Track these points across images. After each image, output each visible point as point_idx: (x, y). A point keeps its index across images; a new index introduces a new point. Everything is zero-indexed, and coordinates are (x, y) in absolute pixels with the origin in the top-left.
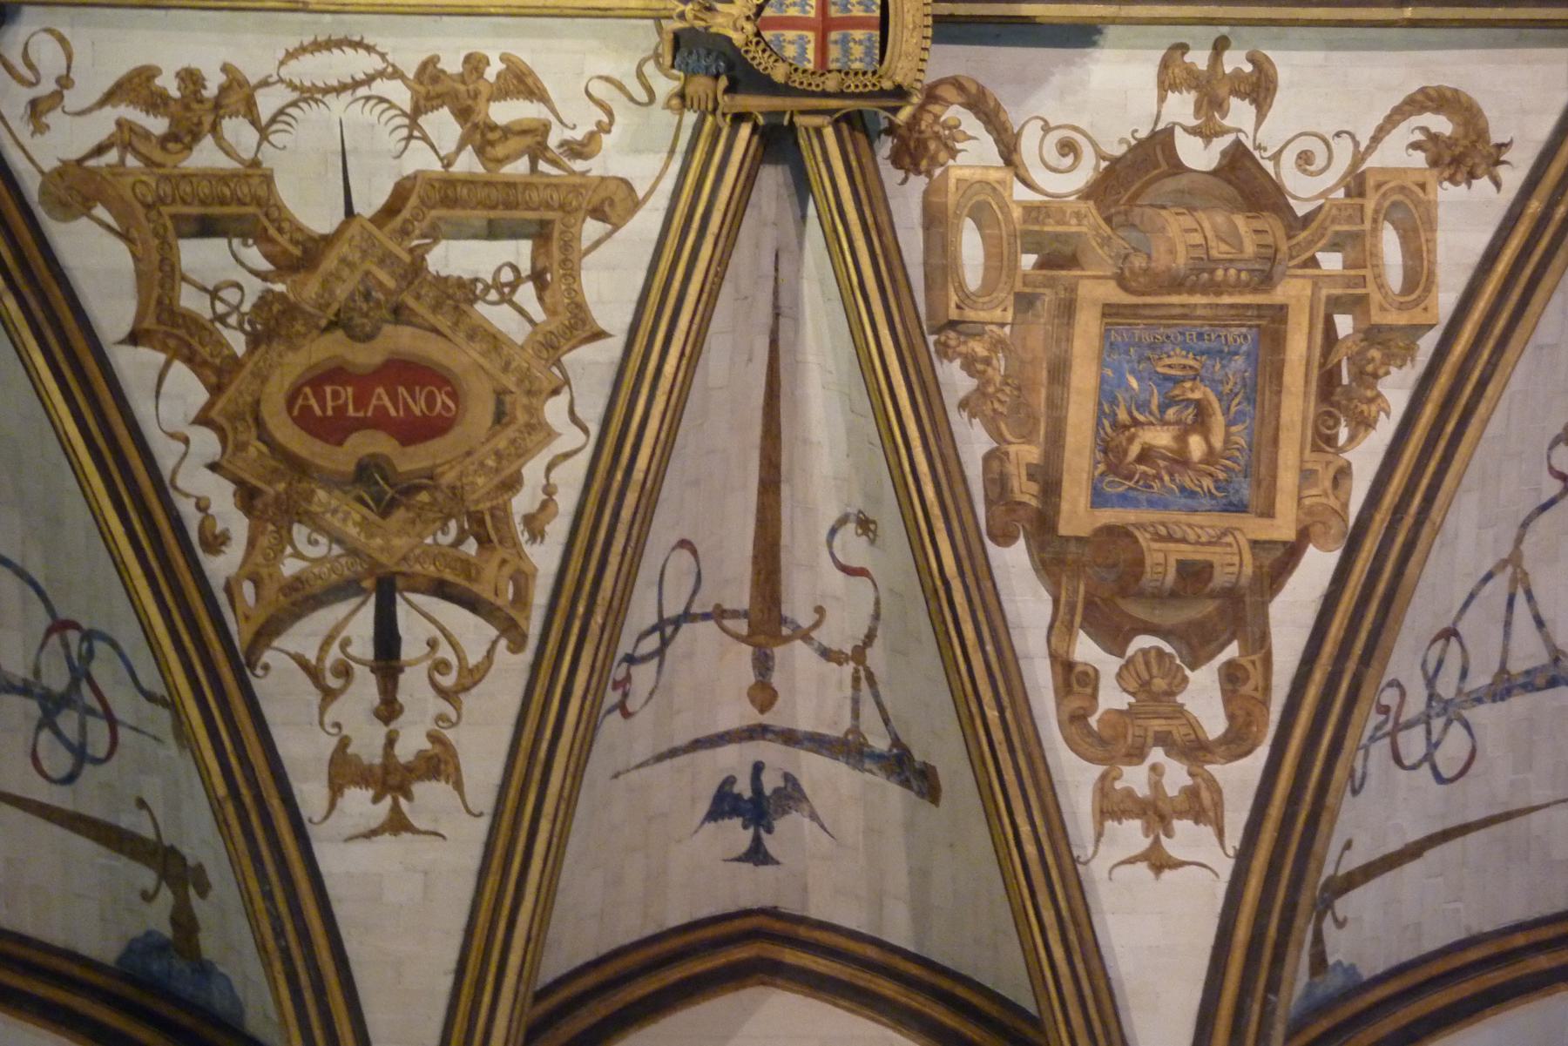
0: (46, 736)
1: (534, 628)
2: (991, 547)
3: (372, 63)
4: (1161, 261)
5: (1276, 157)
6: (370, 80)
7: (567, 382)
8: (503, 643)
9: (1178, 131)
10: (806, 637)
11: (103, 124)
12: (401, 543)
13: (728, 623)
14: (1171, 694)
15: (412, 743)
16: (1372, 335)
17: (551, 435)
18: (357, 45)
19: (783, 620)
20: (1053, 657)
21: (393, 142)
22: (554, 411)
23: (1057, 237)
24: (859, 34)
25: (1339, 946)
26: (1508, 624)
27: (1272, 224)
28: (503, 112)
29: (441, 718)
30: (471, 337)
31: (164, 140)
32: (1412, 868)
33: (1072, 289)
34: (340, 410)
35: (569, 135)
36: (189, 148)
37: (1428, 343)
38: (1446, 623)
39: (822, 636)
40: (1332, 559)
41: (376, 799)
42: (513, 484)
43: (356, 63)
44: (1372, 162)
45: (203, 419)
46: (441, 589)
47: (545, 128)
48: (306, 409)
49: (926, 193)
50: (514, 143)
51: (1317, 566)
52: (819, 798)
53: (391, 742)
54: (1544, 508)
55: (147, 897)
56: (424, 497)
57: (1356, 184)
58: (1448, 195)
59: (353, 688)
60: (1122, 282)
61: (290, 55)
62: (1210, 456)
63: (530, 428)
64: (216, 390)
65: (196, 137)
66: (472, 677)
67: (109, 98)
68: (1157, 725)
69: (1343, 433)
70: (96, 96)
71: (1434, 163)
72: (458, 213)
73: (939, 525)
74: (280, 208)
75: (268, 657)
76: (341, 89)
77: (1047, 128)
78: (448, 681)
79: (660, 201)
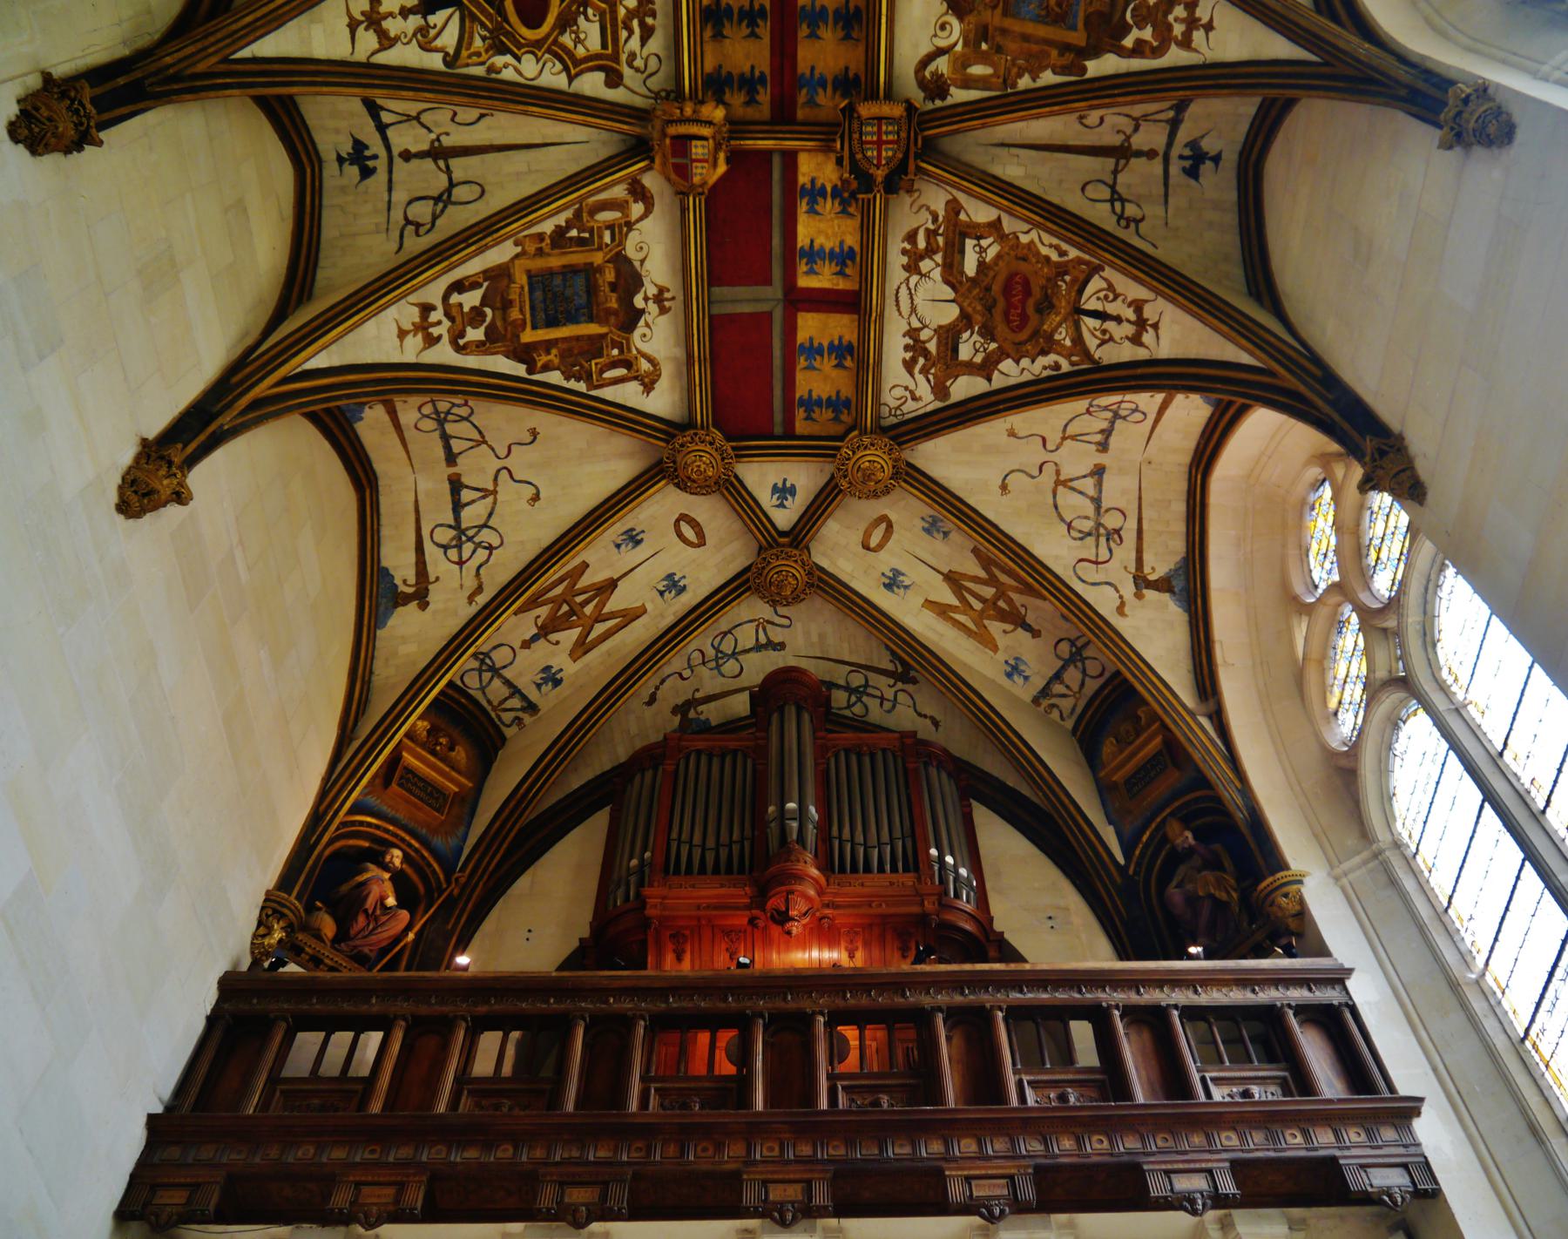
0: (1128, 418)
3: (904, 286)
6: (909, 289)
7: (1014, 233)
8: (1101, 273)
10: (1128, 138)
11: (920, 378)
12: (1063, 304)
13: (1120, 168)
15: (1130, 314)
17: (1032, 242)
19: (1122, 145)
20: (1130, 57)
21: (930, 283)
22: (1024, 239)
23: (976, 34)
24: (884, 128)
28: (922, 244)
29: (1123, 301)
30: (997, 265)
31: (926, 360)
33: (996, 29)
34: (1019, 315)
35: (930, 221)
36: (929, 352)
39: (1129, 131)
41: (1147, 331)
42: (1047, 259)
43: (904, 292)
45: (1017, 362)
46: (1081, 291)
47: (927, 230)
48: (1017, 326)
49: (957, 87)
50: (932, 240)
52: (1197, 134)
56: (1049, 291)
59: (1110, 330)
60: (994, 7)
61: (900, 314)
63: (1029, 249)
64: (1008, 356)
65: (926, 349)
66: (1111, 287)
68: (1160, 15)
70: (911, 379)
72: (956, 263)
74: (950, 324)
75: (1096, 357)
77: (935, 35)
78: (1111, 296)
79: (954, 192)
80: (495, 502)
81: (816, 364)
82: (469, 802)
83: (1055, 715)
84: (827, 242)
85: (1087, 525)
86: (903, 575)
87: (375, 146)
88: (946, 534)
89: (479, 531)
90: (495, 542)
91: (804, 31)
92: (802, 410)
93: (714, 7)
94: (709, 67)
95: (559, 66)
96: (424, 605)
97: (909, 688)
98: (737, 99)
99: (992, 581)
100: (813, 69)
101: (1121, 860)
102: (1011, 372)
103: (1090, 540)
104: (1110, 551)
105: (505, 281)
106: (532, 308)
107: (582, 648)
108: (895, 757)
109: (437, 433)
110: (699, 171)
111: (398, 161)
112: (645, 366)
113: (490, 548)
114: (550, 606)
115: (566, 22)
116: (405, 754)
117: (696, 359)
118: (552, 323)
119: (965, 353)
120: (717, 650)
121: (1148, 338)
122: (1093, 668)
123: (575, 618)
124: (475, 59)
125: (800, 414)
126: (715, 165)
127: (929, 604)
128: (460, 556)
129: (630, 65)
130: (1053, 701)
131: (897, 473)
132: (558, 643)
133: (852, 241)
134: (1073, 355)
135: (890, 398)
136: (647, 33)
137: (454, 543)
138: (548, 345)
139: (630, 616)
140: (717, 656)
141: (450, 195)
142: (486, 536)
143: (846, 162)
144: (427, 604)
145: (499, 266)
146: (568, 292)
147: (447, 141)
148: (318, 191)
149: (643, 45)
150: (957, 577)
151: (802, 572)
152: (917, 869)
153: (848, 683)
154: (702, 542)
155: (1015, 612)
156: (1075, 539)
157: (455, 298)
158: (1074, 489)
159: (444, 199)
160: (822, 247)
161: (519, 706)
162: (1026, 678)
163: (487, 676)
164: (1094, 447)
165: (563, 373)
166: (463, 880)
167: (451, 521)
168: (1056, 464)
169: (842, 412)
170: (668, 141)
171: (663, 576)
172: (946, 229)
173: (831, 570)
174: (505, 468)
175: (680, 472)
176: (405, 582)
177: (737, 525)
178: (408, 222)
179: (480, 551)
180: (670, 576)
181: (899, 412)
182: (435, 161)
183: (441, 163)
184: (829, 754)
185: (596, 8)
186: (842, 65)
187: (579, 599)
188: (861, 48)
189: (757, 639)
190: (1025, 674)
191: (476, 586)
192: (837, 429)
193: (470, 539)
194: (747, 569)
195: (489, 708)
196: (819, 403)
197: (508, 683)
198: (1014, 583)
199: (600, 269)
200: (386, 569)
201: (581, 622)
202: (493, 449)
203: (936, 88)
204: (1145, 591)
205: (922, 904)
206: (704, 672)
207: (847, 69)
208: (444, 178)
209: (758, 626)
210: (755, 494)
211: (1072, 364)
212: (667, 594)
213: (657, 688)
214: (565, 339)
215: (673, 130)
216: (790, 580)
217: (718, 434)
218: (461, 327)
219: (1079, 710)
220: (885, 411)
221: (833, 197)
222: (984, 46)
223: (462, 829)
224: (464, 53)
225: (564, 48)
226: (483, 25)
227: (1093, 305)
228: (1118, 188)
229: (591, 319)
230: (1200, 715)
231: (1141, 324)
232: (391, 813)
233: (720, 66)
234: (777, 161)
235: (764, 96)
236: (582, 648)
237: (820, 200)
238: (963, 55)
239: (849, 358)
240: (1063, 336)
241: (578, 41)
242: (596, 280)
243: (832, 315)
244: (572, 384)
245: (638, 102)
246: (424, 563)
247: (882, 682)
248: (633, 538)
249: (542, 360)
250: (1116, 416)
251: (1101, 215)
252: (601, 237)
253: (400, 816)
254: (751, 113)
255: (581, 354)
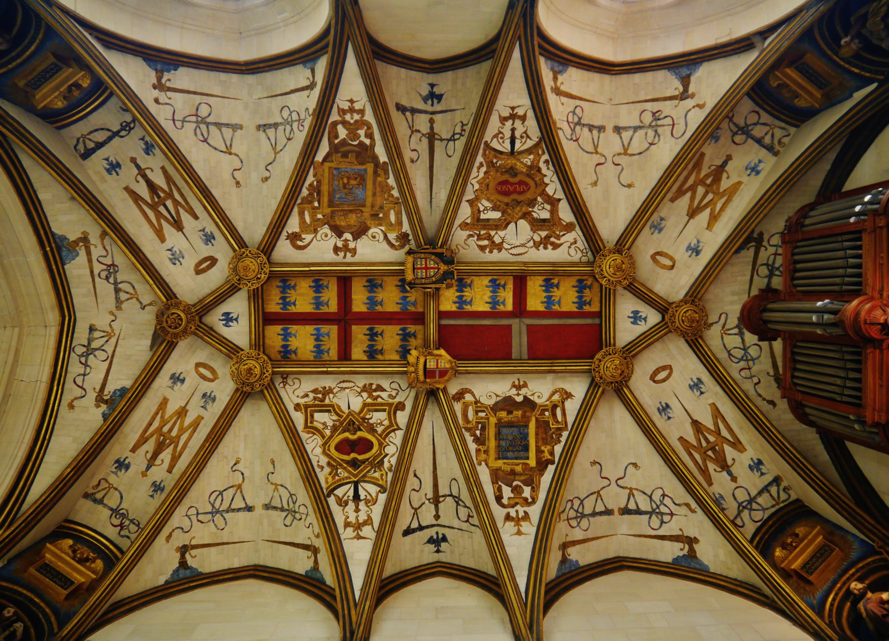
1: (482, 146)
2: (387, 161)
3: (511, 251)
4: (354, 216)
5: (332, 236)
9: (352, 240)
10: (423, 135)
11: (563, 240)
14: (349, 133)
15: (509, 124)
16: (311, 202)
17: (478, 182)
18: (513, 255)
19: (428, 138)
20: (374, 140)
22: (477, 187)
24: (419, 266)
25: (308, 73)
26: (276, 140)
27: (332, 223)
28: (486, 242)
30: (493, 200)
31: (551, 237)
32: (293, 88)
33: (372, 210)
34: (520, 186)
37: (299, 201)
38: (290, 142)
39: (419, 135)
40: (316, 159)
42: (485, 173)
43: (513, 251)
44: (313, 235)
45: (547, 185)
46: (501, 153)
47: (477, 240)
50: (483, 237)
51: (319, 157)
52: (419, 99)
53: (513, 124)
54: (270, 164)
55: (562, 83)
56: (504, 170)
57: (315, 231)
58: (297, 230)
60: (362, 211)
62: (342, 179)
63: (482, 183)
64: (544, 190)
65: (545, 237)
66: (496, 136)
67: (561, 244)
68: (352, 127)
69: (315, 183)
71: (300, 236)
73: (400, 169)
75: (537, 140)
76: (516, 247)
78: (501, 135)
79: (455, 226)
80: (637, 489)
81: (557, 299)
82: (831, 530)
83: (786, 140)
84: (487, 294)
85: (651, 133)
86: (690, 244)
87: (431, 532)
88: (662, 219)
89: (655, 503)
90: (660, 492)
91: (379, 308)
92: (585, 308)
93: (368, 354)
94: (397, 357)
95: (392, 434)
96: (696, 540)
97: (766, 237)
98: (413, 342)
99: (693, 189)
100: (397, 303)
101: (874, 86)
102: (554, 188)
103: (660, 130)
104: (666, 117)
105: (500, 472)
106: (516, 458)
107: (737, 444)
108: (797, 247)
109: (590, 519)
110: (443, 364)
111: (440, 522)
112: (556, 397)
113: (664, 495)
114: (708, 462)
115: (372, 429)
116: (793, 567)
117: (550, 368)
118: (526, 448)
119: (545, 215)
120: (741, 359)
121: (520, 112)
122: (753, 118)
123: (717, 448)
124: (384, 477)
125: (587, 308)
126: (440, 356)
127: (709, 227)
128: (668, 514)
129: (394, 398)
130: (776, 142)
131: (618, 251)
132: (733, 459)
133: (486, 281)
134: (538, 154)
135: (576, 256)
136: (380, 388)
137: (660, 517)
138: (539, 451)
139: (717, 414)
140: (745, 360)
141: (456, 497)
142: (657, 497)
143: (437, 286)
144: (695, 538)
145: (491, 475)
146: (510, 438)
147: (430, 495)
148: (451, 566)
149: (386, 391)
150: (691, 211)
151: (683, 307)
152: (860, 232)
153: (766, 277)
154: (670, 367)
155: (714, 173)
156: (659, 140)
157: (505, 501)
158: (629, 143)
159: (457, 500)
160: (491, 297)
161: (776, 488)
162: (760, 161)
163: (755, 506)
164: (602, 135)
165: (556, 444)
166: (880, 543)
167: (648, 516)
168: (614, 156)
169: (586, 284)
170: (428, 380)
171: (690, 391)
172: (476, 229)
173: (687, 289)
174: (616, 481)
175: (619, 379)
176: (682, 550)
177: (658, 346)
178: (467, 521)
179: (665, 502)
180: (691, 387)
181: (585, 251)
182: (440, 502)
183: (441, 499)
184: (794, 291)
185: (366, 414)
186: (394, 288)
187: (704, 444)
188: (385, 278)
189: (735, 334)
190: (757, 162)
191: (685, 507)
192: (596, 286)
193: (658, 507)
194: (687, 341)
195: (777, 507)
196: (580, 298)
197: (760, 493)
198: (694, 174)
199: (499, 420)
200: (674, 559)
201: (720, 444)
202: (604, 488)
203: (404, 238)
204: (690, 92)
205: (881, 228)
206: (755, 369)
207: (397, 286)
208: (448, 498)
209: (726, 334)
210: (638, 335)
211: (544, 153)
212: (702, 390)
213: (764, 399)
214: (537, 442)
215: (422, 378)
216: (687, 314)
217: (598, 356)
218: (521, 500)
219: (783, 125)
220: (584, 259)
221: (462, 291)
222: (381, 215)
223: (850, 538)
224: (380, 482)
225: (384, 431)
226: (368, 472)
227: (507, 146)
228: (449, 138)
229: (527, 426)
230: (763, 45)
231: (513, 117)
232: (829, 584)
233: (397, 351)
234: (444, 322)
235: (412, 328)
236: (737, 444)
237: (464, 299)
238: (386, 226)
239: (553, 281)
240: (528, 160)
241: (381, 424)
242: (505, 422)
243: (528, 291)
244: (563, 439)
245: (413, 393)
246: (671, 536)
247: (764, 255)
248: (665, 409)
249: (547, 456)
250: (579, 123)
251: (460, 144)
252: (482, 418)
253: (832, 578)
254: (420, 336)
255: (546, 433)
